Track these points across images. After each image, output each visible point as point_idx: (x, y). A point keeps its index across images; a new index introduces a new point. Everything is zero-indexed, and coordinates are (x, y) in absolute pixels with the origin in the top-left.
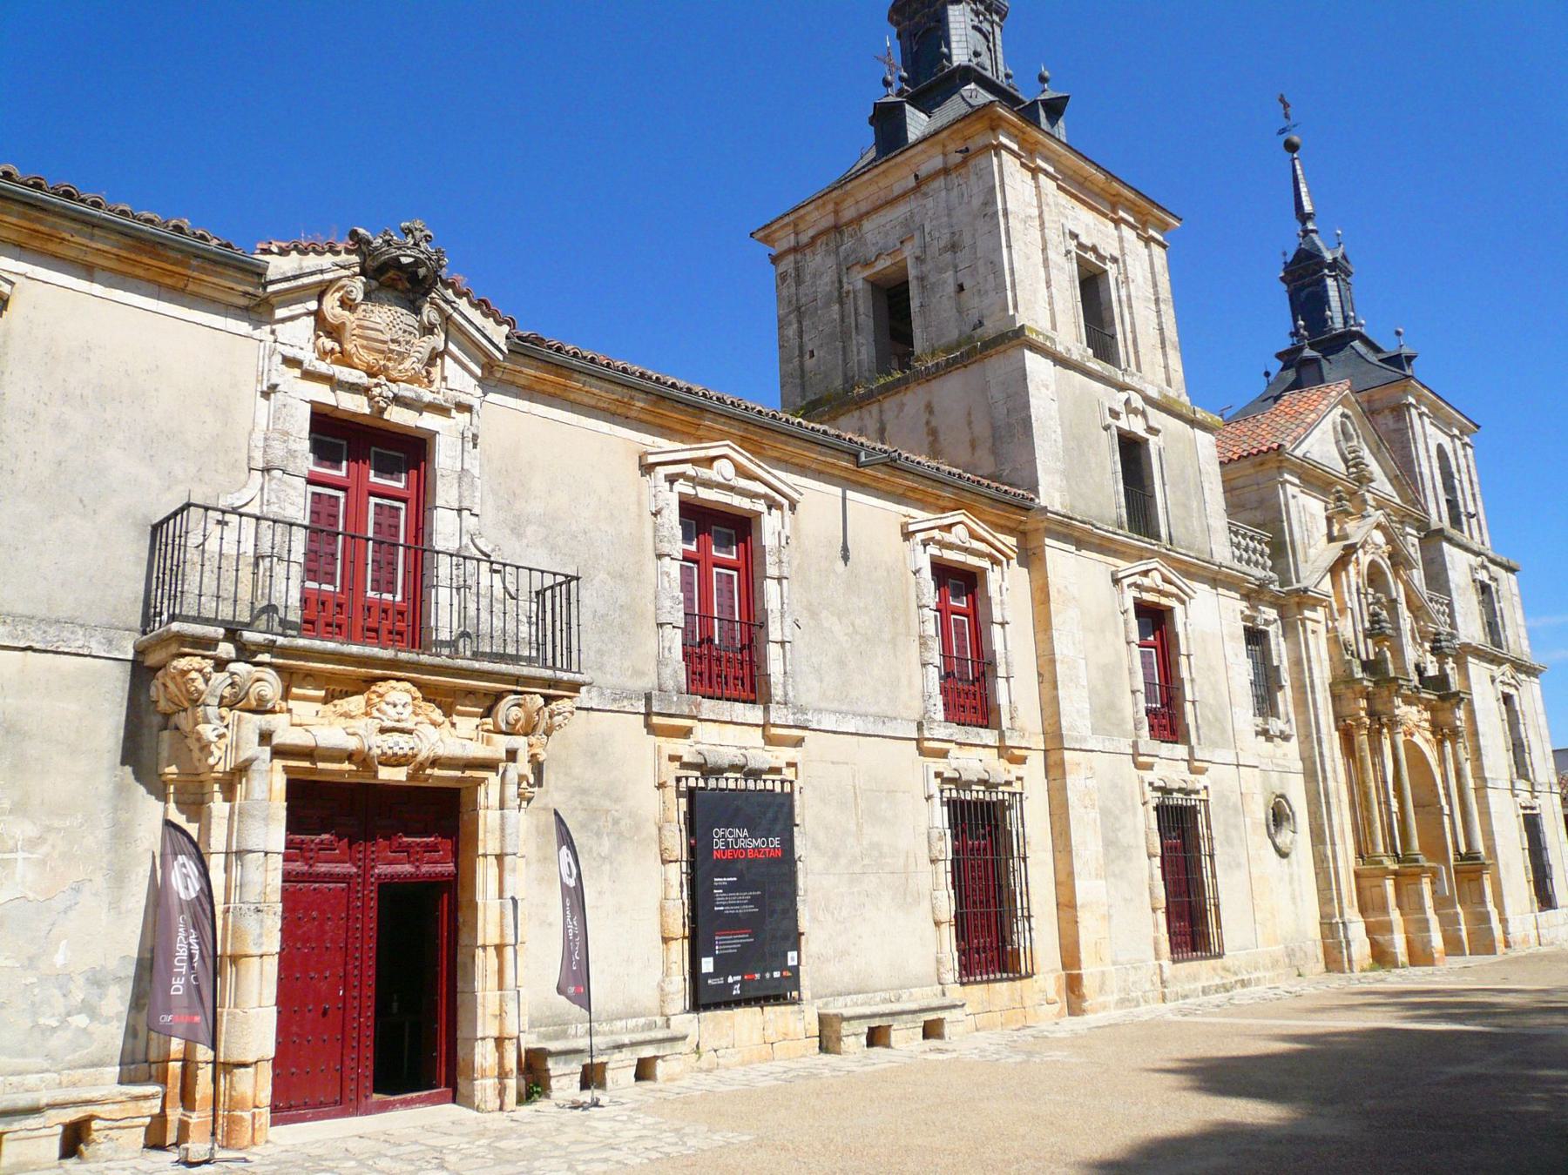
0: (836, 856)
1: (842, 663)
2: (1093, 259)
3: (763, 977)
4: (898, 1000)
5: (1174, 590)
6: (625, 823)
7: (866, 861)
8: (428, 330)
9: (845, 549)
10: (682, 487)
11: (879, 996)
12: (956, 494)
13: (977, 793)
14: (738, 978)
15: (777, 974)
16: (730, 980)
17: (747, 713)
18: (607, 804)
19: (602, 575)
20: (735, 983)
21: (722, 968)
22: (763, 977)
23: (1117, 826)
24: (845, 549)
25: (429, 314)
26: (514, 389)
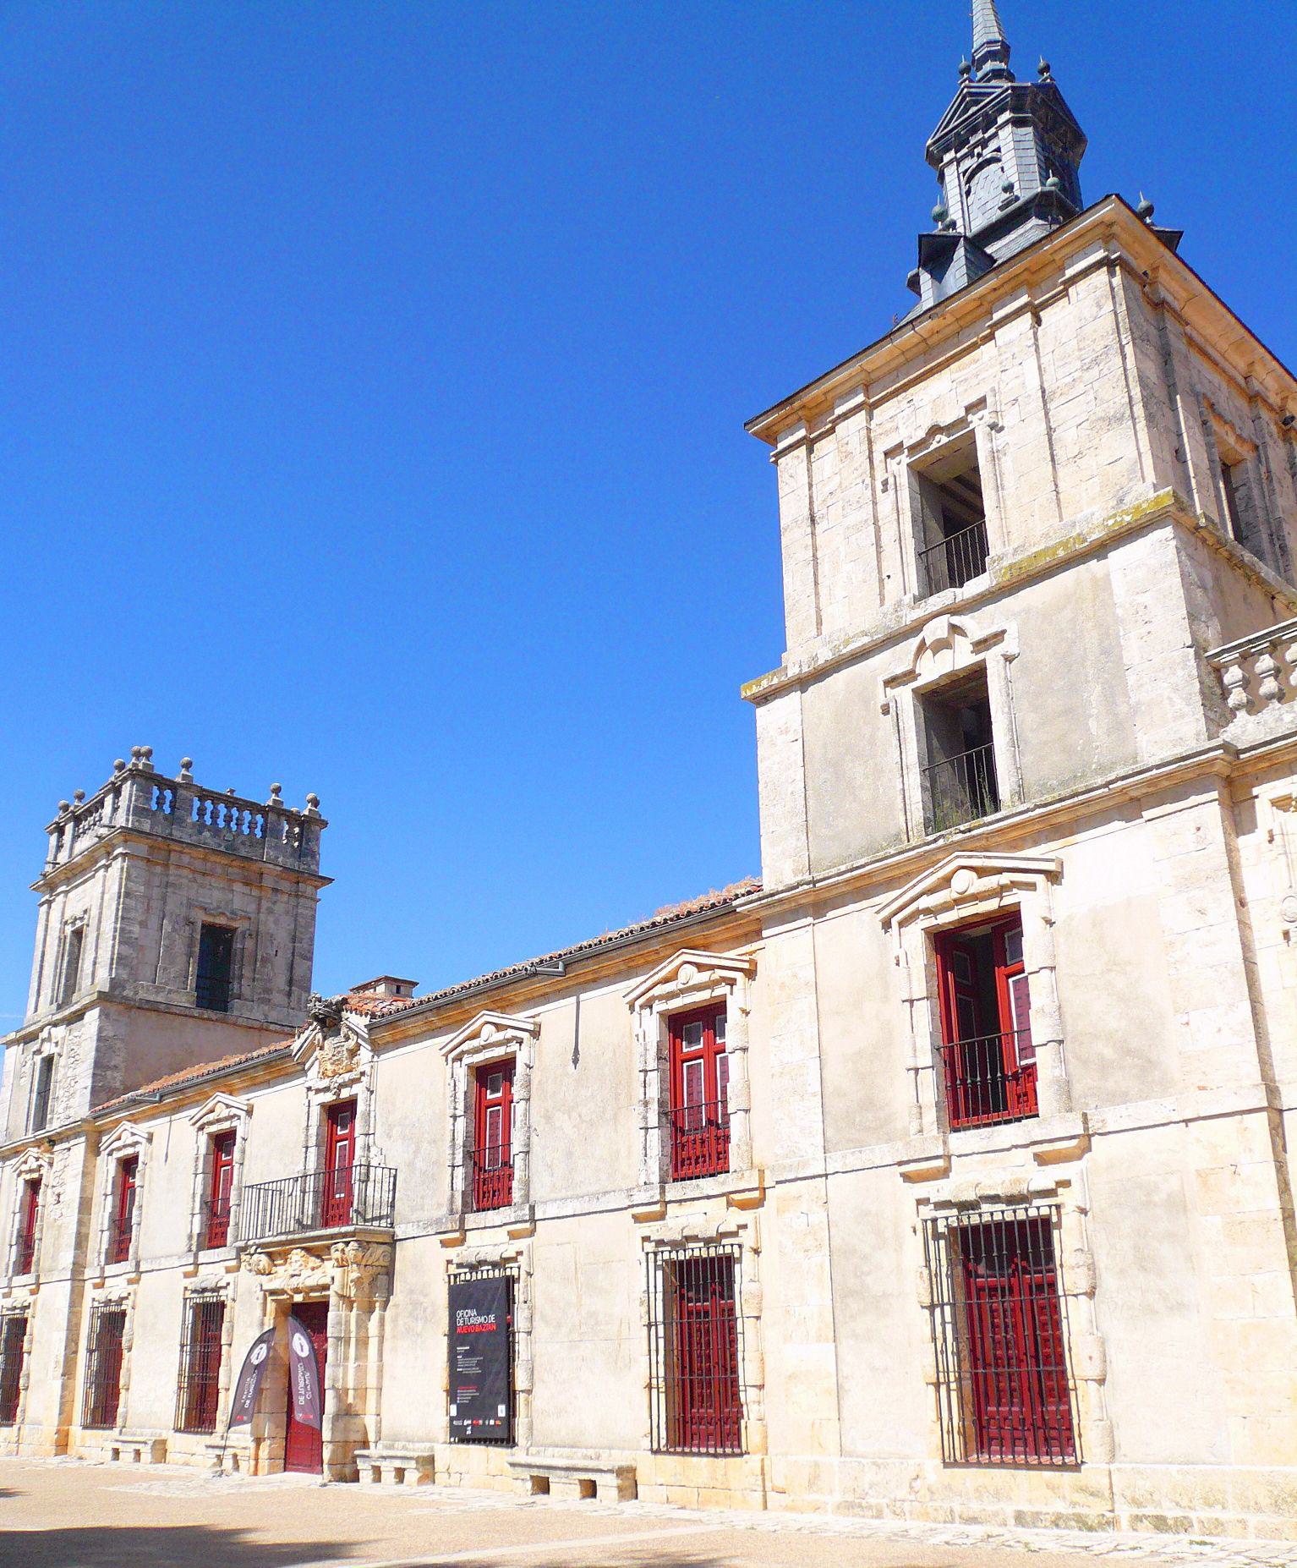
0: (559, 1325)
1: (570, 1154)
2: (944, 439)
3: (484, 1423)
4: (598, 1458)
5: (1005, 878)
6: (429, 1310)
7: (584, 1329)
8: (347, 1038)
9: (576, 1051)
10: (467, 1060)
11: (581, 1452)
12: (662, 942)
13: (697, 1250)
14: (470, 1422)
15: (492, 1422)
16: (466, 1423)
17: (495, 1217)
18: (422, 1299)
19: (426, 1144)
20: (468, 1425)
21: (461, 1414)
22: (484, 1423)
23: (865, 1269)
24: (576, 1051)
25: (344, 1030)
26: (391, 1045)
